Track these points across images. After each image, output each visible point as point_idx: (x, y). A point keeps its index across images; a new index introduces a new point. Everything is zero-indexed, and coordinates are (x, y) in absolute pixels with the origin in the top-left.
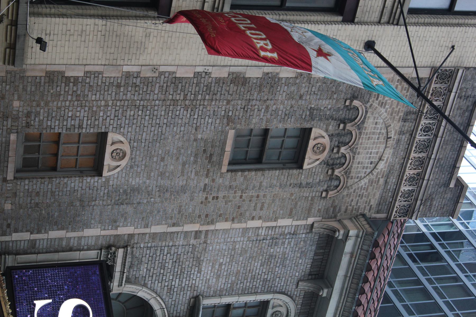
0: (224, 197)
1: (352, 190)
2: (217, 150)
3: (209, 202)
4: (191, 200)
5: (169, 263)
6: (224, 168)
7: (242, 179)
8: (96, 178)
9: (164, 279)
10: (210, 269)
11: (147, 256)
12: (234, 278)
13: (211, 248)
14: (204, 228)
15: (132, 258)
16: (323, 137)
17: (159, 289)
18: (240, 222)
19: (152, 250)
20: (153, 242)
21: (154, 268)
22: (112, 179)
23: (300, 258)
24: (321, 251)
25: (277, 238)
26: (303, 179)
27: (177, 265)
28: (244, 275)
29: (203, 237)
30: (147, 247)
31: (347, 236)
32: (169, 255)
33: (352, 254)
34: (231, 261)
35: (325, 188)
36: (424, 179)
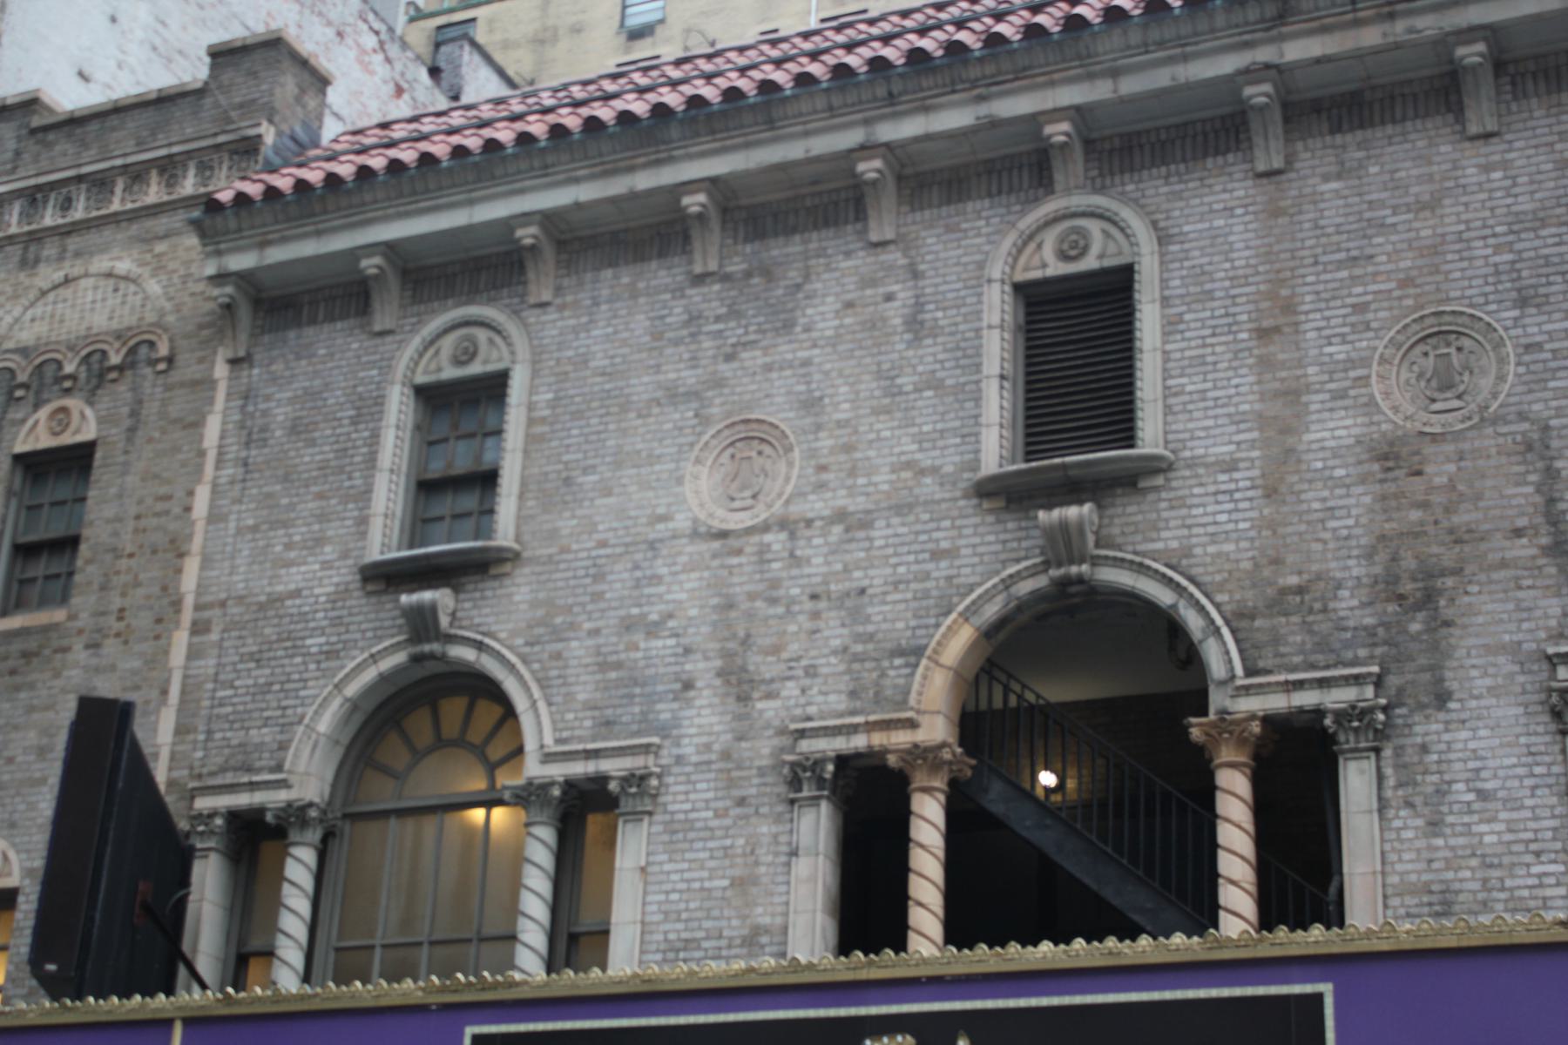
0: (124, 595)
1: (168, 306)
2: (17, 646)
3: (128, 626)
4: (113, 668)
5: (256, 677)
6: (59, 615)
7: (91, 569)
8: (21, 899)
9: (296, 676)
10: (294, 570)
11: (229, 734)
12: (333, 502)
13: (241, 585)
14: (187, 616)
15: (223, 770)
16: (37, 422)
17: (322, 682)
18: (190, 537)
19: (214, 726)
20: (195, 730)
21: (262, 710)
22: (28, 864)
23: (314, 355)
24: (305, 311)
25: (250, 434)
26: (116, 433)
27: (266, 655)
28: (331, 478)
29: (206, 614)
30: (206, 740)
31: (220, 278)
32: (237, 683)
33: (263, 245)
34: (285, 524)
35: (148, 371)
36: (170, 156)
